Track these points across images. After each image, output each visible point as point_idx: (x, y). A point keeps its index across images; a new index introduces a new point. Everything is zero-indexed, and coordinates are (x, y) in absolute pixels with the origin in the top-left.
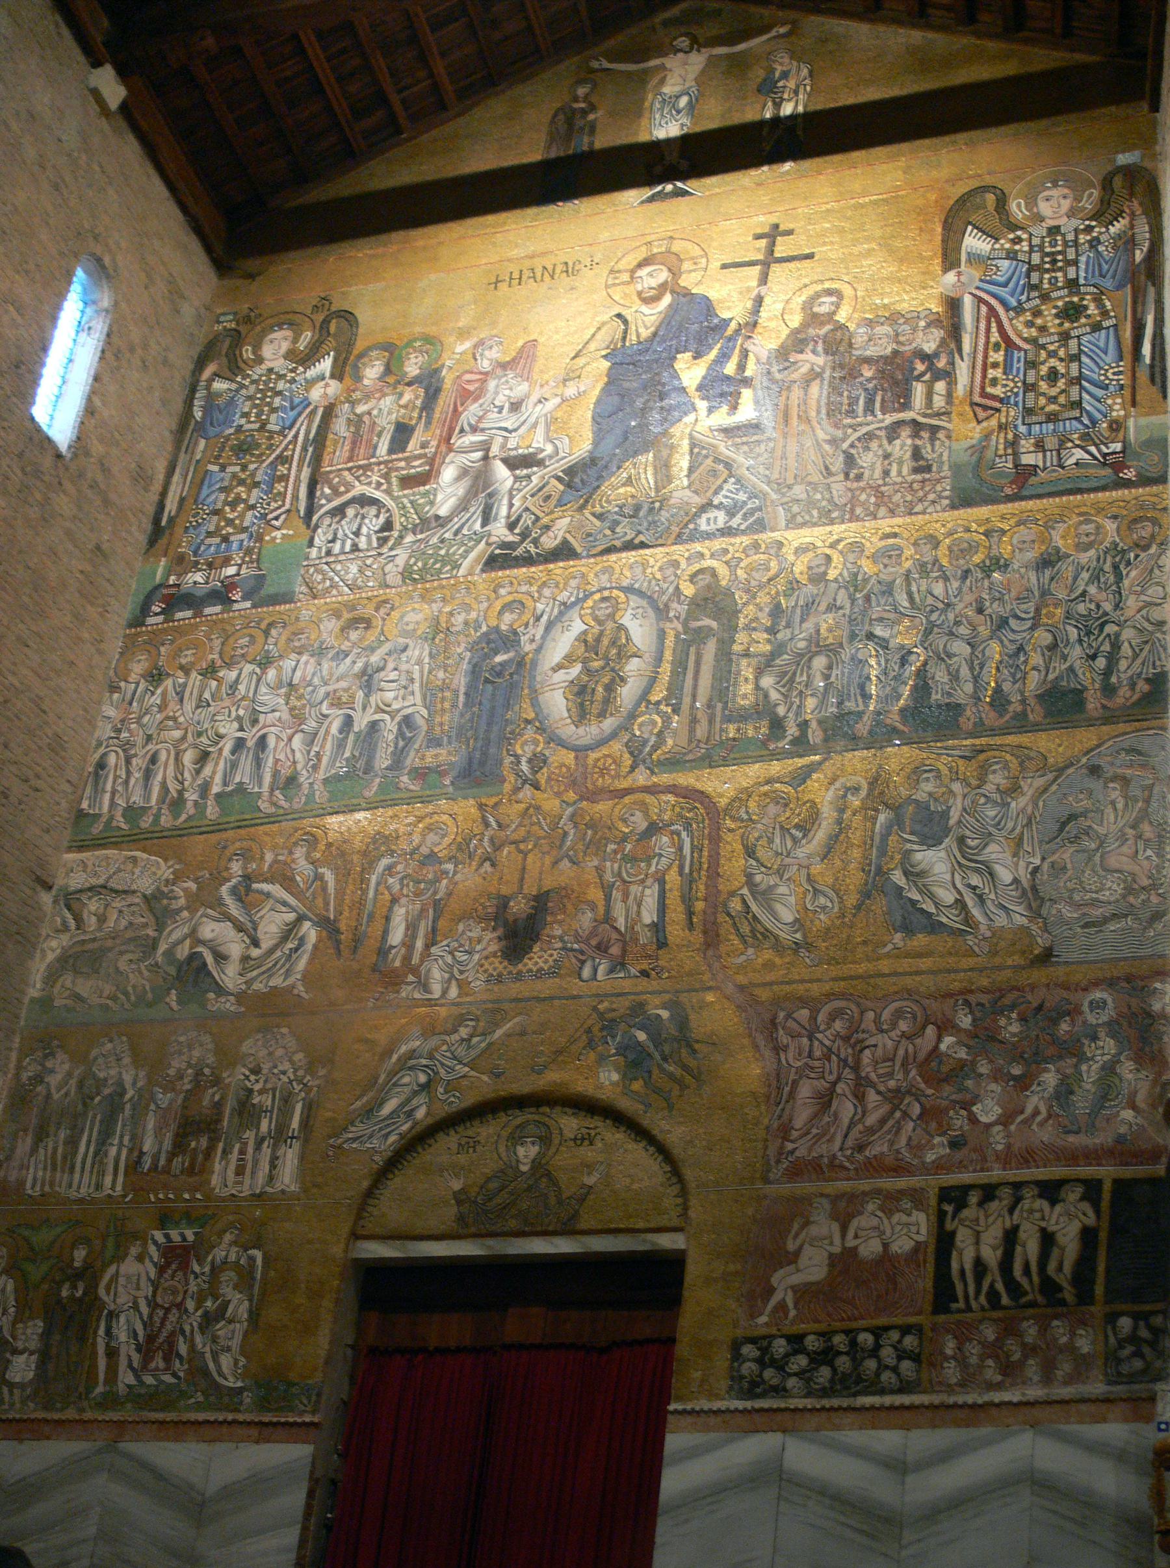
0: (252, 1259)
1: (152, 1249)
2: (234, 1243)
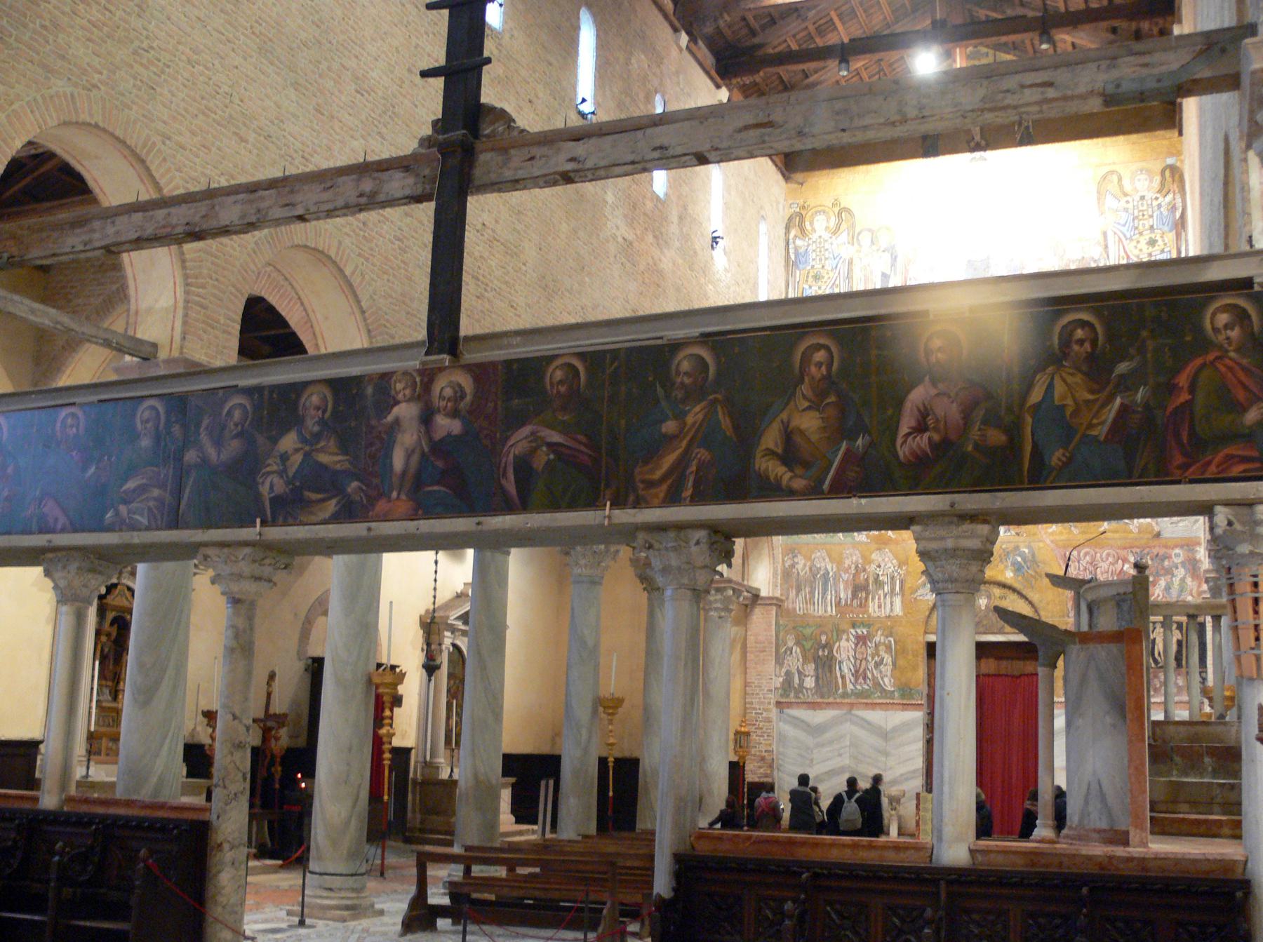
0: (890, 641)
1: (851, 637)
2: (882, 635)
